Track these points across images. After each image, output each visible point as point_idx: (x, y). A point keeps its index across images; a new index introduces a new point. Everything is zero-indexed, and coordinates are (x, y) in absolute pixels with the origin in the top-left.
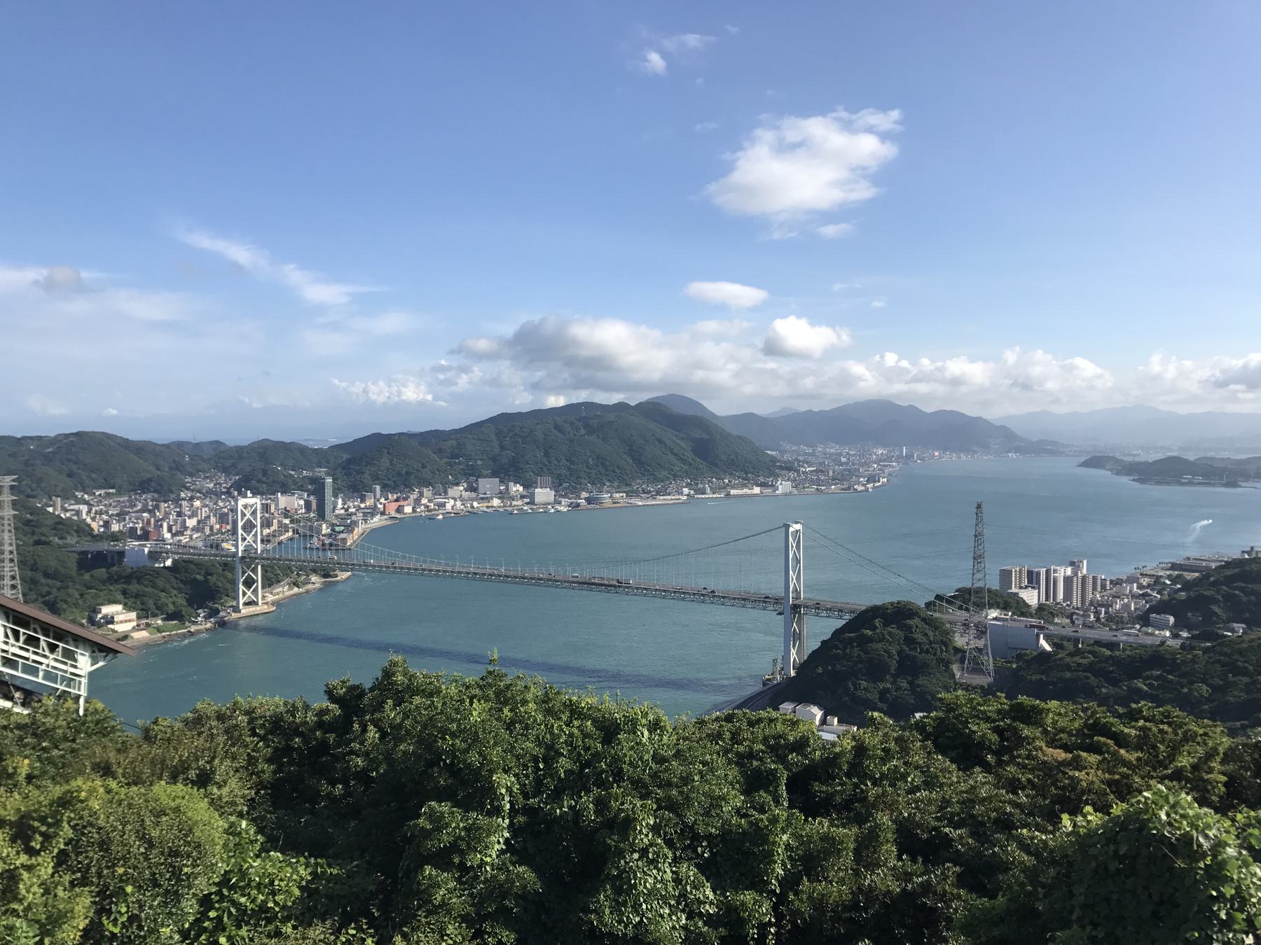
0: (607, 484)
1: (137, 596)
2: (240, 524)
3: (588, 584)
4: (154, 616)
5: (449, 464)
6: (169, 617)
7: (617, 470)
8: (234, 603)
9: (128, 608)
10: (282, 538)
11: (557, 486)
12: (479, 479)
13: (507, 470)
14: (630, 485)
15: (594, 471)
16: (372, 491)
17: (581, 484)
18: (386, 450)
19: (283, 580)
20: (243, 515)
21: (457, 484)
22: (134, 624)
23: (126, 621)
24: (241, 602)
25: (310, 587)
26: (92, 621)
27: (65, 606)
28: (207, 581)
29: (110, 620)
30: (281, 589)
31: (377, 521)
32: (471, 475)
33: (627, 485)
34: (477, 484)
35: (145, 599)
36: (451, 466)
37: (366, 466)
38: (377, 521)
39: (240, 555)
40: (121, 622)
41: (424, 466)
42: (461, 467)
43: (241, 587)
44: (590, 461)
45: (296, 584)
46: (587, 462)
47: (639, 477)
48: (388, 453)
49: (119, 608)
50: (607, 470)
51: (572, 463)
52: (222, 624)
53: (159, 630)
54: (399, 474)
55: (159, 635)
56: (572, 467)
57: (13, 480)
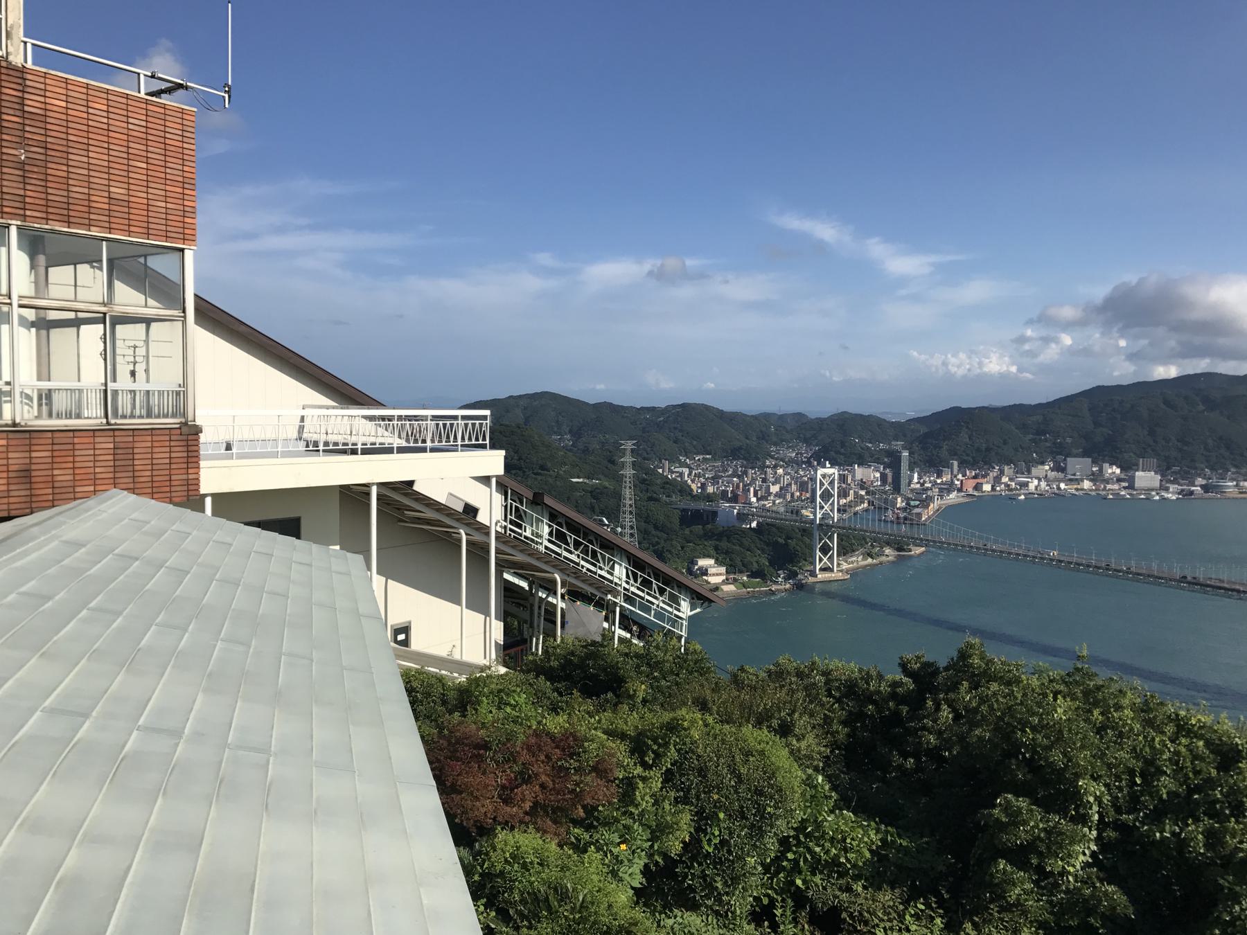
0: (1233, 470)
1: (727, 553)
2: (819, 493)
3: (1201, 585)
4: (741, 572)
5: (1033, 440)
6: (753, 575)
8: (810, 568)
9: (719, 563)
10: (858, 508)
11: (1164, 470)
12: (1068, 459)
13: (1100, 451)
16: (950, 467)
19: (858, 550)
20: (822, 484)
21: (1043, 463)
22: (724, 577)
23: (717, 575)
24: (818, 567)
25: (883, 559)
26: (690, 572)
27: (669, 556)
28: (787, 544)
29: (704, 572)
30: (855, 559)
31: (953, 497)
32: (1058, 454)
34: (1066, 464)
35: (733, 555)
36: (1036, 443)
38: (953, 497)
39: (818, 522)
40: (714, 575)
41: (1005, 443)
42: (1048, 444)
43: (818, 553)
45: (870, 555)
48: (967, 427)
49: (712, 562)
50: (1231, 453)
52: (800, 586)
53: (744, 585)
54: (978, 450)
55: (744, 590)
56: (1185, 448)
57: (633, 445)
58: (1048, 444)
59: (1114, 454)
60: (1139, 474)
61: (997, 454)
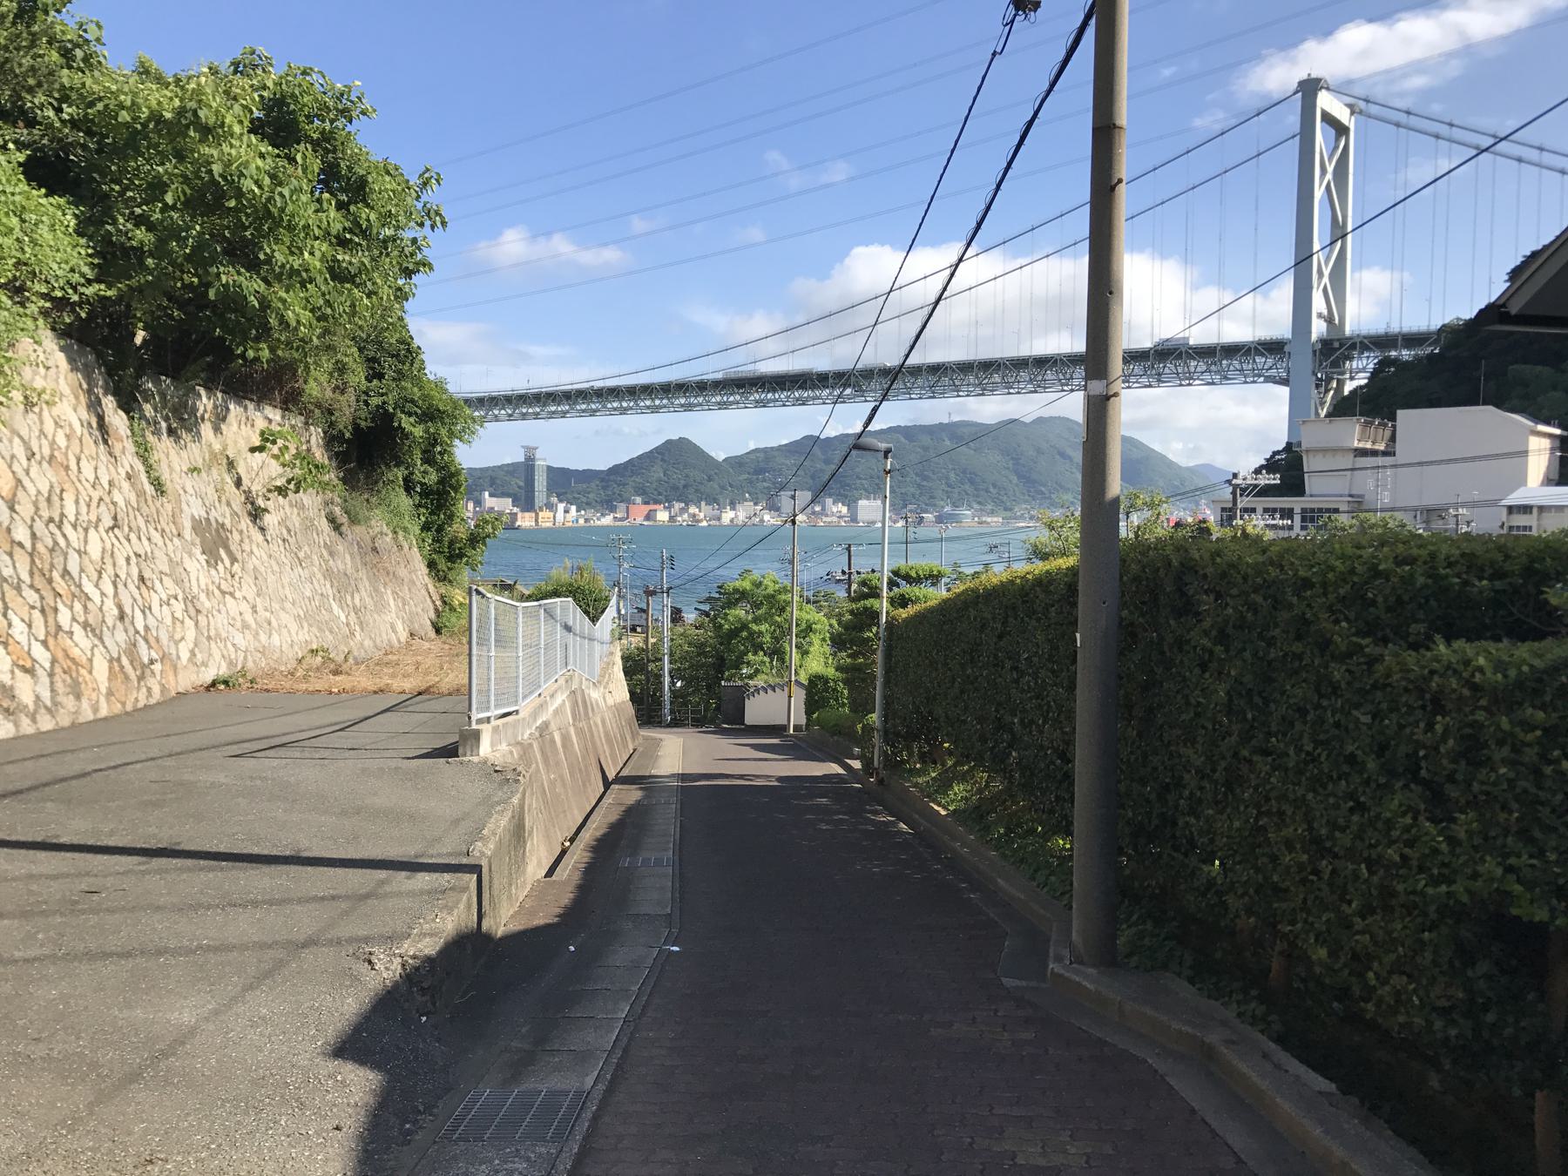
7: (992, 490)
14: (1011, 510)
15: (956, 490)
17: (935, 505)
18: (660, 457)
33: (1006, 509)
36: (751, 482)
37: (631, 476)
42: (765, 484)
44: (952, 475)
46: (947, 478)
47: (1026, 502)
48: (662, 460)
51: (925, 478)
56: (925, 483)
58: (765, 484)
59: (842, 491)
60: (862, 503)
61: (697, 491)
